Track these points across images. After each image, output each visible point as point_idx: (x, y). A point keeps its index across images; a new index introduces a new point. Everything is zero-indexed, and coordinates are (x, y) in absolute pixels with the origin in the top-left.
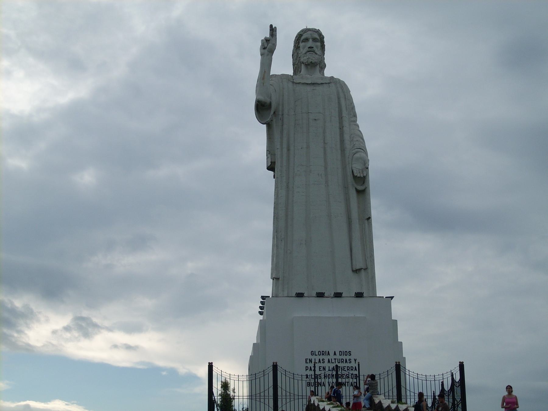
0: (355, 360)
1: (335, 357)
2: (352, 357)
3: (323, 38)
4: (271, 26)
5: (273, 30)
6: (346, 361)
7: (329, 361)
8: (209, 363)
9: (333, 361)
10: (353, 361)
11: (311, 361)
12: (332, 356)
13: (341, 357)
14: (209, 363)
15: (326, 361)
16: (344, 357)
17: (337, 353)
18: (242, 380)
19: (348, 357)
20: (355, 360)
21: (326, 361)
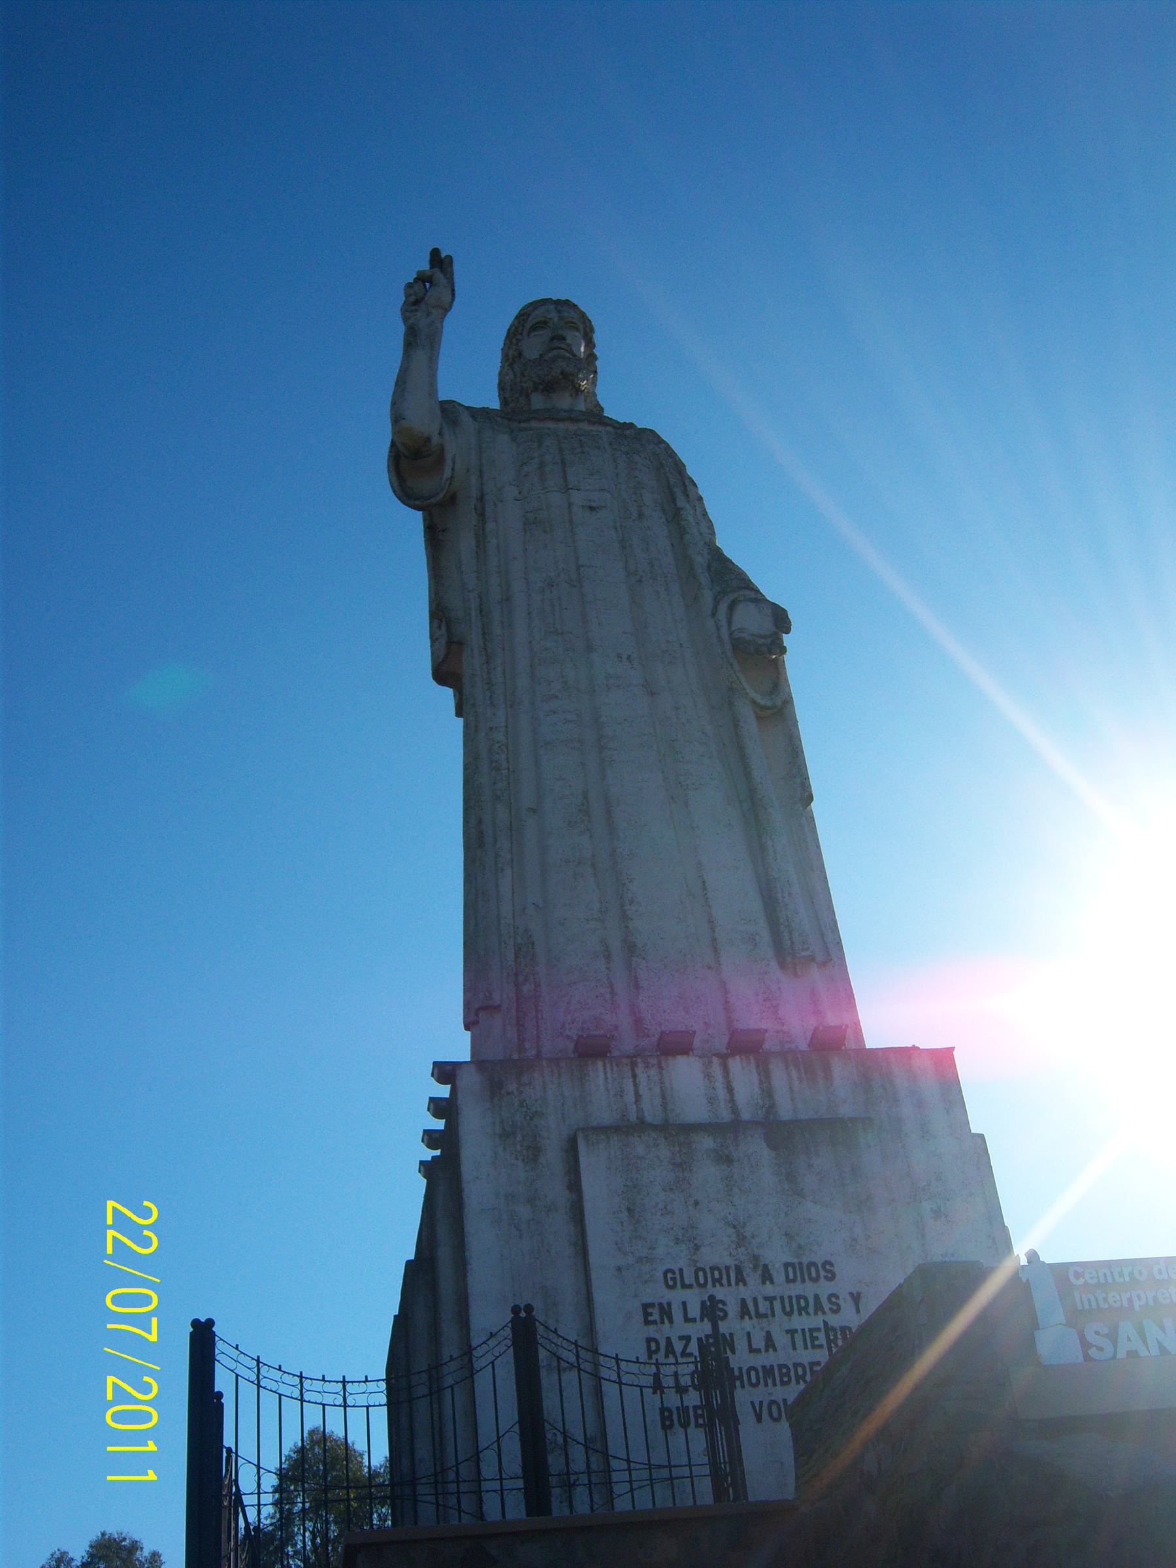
0: (856, 1298)
1: (769, 1290)
2: (843, 1286)
3: (592, 330)
4: (435, 253)
5: (440, 262)
6: (819, 1308)
7: (744, 1312)
8: (196, 1323)
9: (763, 1307)
10: (847, 1305)
11: (666, 1312)
12: (753, 1288)
13: (796, 1289)
14: (196, 1323)
15: (733, 1309)
16: (808, 1289)
17: (779, 1277)
18: (362, 1400)
19: (824, 1289)
20: (856, 1298)
21: (733, 1309)
